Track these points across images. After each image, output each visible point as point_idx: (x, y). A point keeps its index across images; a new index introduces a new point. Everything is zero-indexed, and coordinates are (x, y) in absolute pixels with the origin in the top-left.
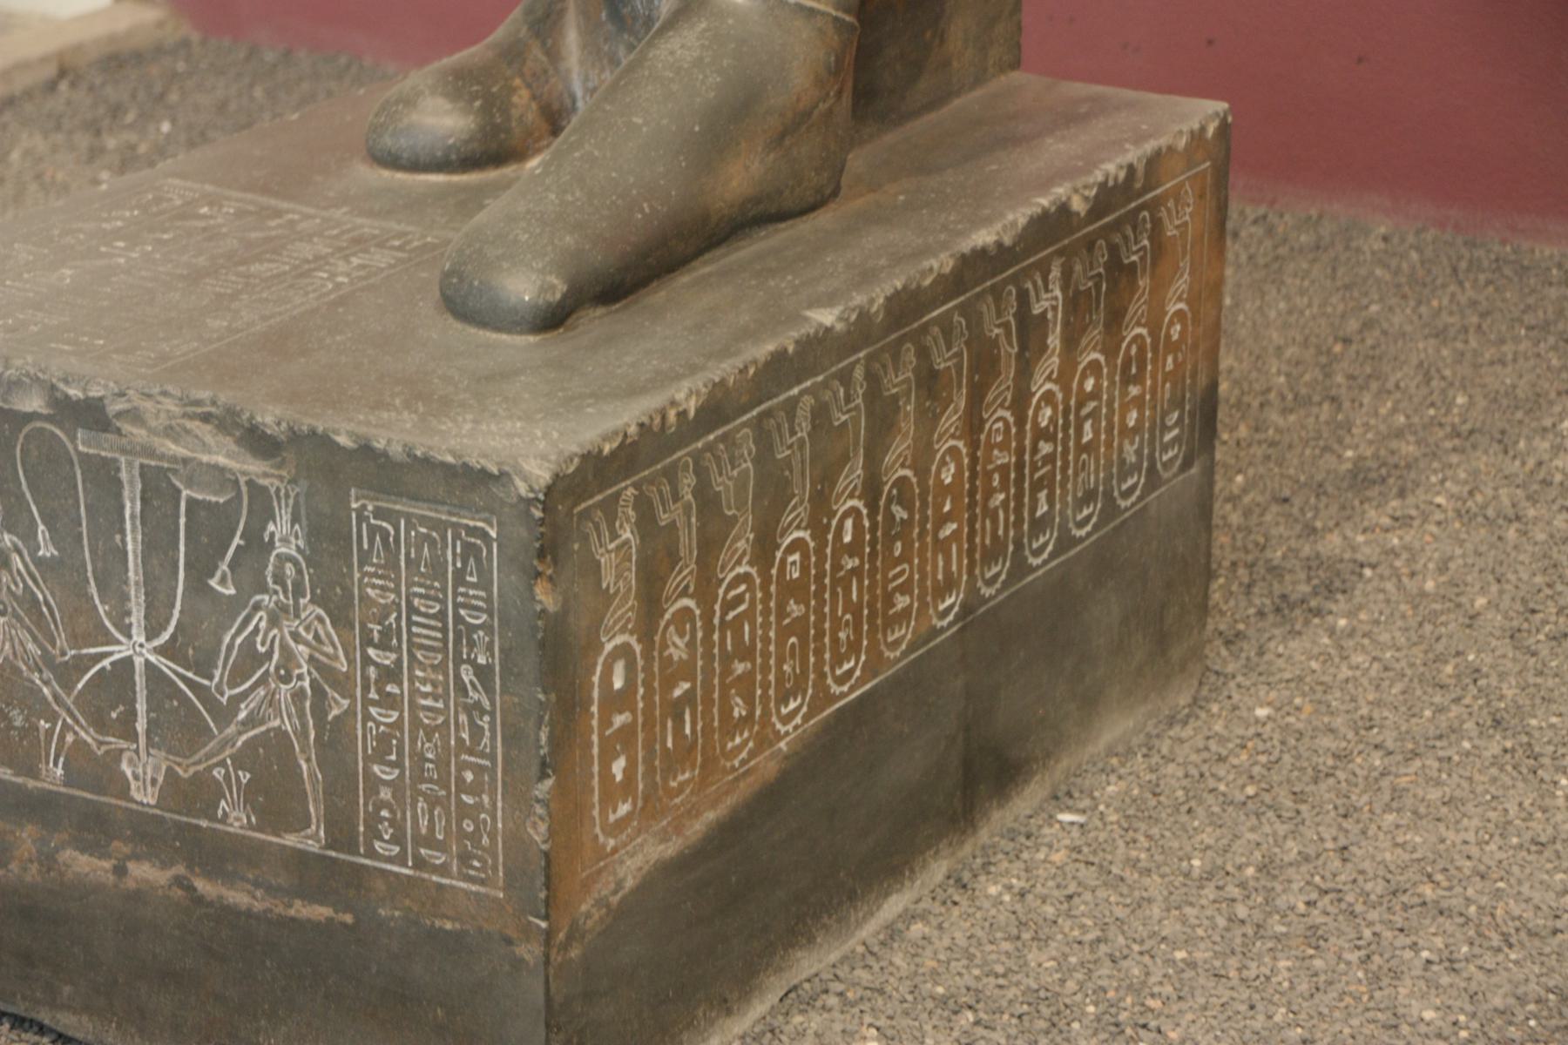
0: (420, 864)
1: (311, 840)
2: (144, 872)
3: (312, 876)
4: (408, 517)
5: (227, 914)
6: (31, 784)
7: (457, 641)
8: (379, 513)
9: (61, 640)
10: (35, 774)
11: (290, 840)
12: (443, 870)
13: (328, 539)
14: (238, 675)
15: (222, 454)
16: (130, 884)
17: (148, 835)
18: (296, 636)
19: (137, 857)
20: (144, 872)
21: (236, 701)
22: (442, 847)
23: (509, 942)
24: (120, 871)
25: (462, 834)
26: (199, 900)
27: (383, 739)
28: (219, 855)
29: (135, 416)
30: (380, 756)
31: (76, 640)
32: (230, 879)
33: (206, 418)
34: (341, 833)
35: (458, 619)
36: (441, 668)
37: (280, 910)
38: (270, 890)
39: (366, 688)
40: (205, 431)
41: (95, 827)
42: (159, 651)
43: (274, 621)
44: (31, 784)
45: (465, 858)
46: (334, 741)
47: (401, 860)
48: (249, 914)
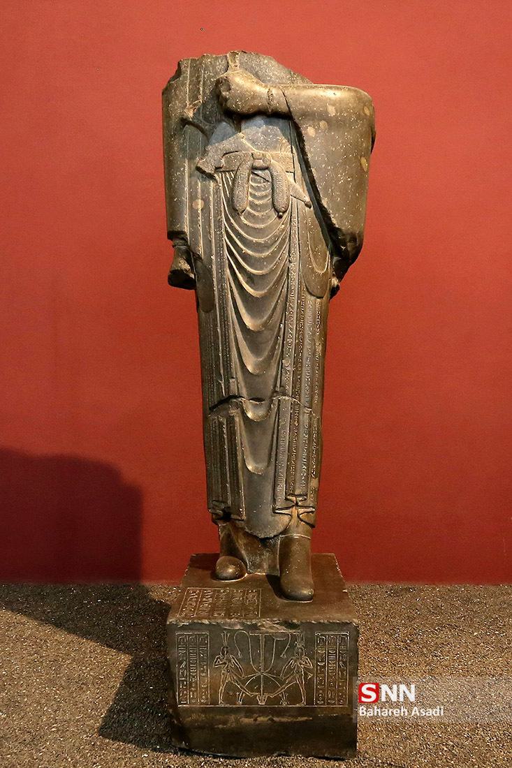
0: (328, 704)
1: (303, 704)
2: (261, 719)
3: (301, 712)
4: (328, 635)
5: (282, 723)
6: (234, 706)
7: (339, 657)
8: (322, 635)
9: (243, 675)
10: (235, 704)
11: (298, 705)
12: (334, 704)
13: (310, 643)
14: (287, 673)
15: (282, 630)
16: (257, 722)
17: (262, 711)
18: (301, 664)
19: (260, 716)
20: (261, 719)
21: (285, 680)
22: (334, 699)
23: (349, 715)
24: (256, 720)
25: (338, 696)
26: (275, 722)
27: (321, 681)
28: (281, 712)
29: (263, 626)
30: (320, 684)
31: (246, 674)
32: (283, 716)
33: (277, 624)
34: (310, 701)
35: (339, 652)
36: (335, 663)
37: (295, 720)
38: (293, 716)
39: (317, 671)
40: (277, 626)
41: (249, 712)
42: (268, 673)
43: (295, 661)
44: (234, 706)
45: (339, 701)
46: (309, 684)
47: (324, 704)
48: (287, 722)
